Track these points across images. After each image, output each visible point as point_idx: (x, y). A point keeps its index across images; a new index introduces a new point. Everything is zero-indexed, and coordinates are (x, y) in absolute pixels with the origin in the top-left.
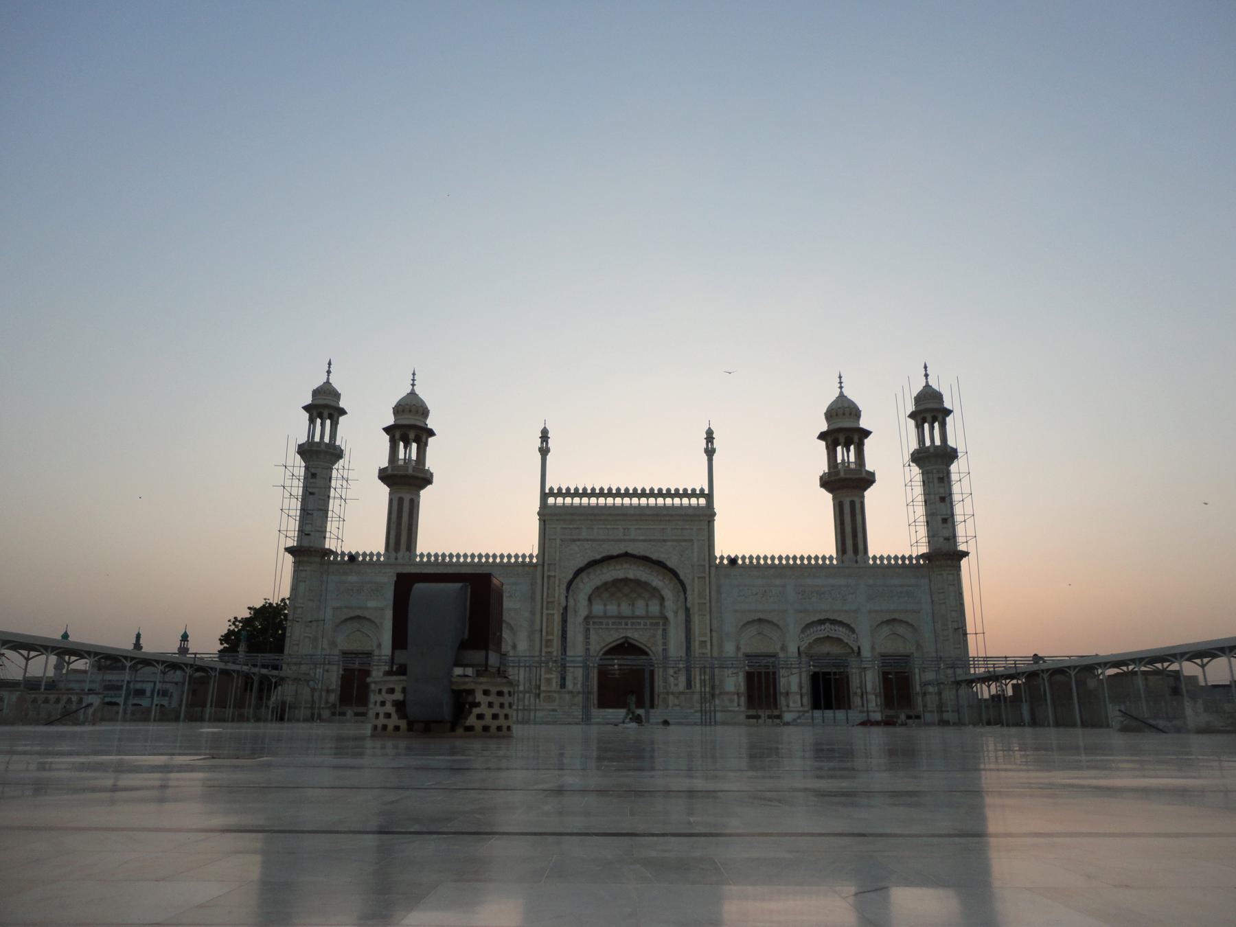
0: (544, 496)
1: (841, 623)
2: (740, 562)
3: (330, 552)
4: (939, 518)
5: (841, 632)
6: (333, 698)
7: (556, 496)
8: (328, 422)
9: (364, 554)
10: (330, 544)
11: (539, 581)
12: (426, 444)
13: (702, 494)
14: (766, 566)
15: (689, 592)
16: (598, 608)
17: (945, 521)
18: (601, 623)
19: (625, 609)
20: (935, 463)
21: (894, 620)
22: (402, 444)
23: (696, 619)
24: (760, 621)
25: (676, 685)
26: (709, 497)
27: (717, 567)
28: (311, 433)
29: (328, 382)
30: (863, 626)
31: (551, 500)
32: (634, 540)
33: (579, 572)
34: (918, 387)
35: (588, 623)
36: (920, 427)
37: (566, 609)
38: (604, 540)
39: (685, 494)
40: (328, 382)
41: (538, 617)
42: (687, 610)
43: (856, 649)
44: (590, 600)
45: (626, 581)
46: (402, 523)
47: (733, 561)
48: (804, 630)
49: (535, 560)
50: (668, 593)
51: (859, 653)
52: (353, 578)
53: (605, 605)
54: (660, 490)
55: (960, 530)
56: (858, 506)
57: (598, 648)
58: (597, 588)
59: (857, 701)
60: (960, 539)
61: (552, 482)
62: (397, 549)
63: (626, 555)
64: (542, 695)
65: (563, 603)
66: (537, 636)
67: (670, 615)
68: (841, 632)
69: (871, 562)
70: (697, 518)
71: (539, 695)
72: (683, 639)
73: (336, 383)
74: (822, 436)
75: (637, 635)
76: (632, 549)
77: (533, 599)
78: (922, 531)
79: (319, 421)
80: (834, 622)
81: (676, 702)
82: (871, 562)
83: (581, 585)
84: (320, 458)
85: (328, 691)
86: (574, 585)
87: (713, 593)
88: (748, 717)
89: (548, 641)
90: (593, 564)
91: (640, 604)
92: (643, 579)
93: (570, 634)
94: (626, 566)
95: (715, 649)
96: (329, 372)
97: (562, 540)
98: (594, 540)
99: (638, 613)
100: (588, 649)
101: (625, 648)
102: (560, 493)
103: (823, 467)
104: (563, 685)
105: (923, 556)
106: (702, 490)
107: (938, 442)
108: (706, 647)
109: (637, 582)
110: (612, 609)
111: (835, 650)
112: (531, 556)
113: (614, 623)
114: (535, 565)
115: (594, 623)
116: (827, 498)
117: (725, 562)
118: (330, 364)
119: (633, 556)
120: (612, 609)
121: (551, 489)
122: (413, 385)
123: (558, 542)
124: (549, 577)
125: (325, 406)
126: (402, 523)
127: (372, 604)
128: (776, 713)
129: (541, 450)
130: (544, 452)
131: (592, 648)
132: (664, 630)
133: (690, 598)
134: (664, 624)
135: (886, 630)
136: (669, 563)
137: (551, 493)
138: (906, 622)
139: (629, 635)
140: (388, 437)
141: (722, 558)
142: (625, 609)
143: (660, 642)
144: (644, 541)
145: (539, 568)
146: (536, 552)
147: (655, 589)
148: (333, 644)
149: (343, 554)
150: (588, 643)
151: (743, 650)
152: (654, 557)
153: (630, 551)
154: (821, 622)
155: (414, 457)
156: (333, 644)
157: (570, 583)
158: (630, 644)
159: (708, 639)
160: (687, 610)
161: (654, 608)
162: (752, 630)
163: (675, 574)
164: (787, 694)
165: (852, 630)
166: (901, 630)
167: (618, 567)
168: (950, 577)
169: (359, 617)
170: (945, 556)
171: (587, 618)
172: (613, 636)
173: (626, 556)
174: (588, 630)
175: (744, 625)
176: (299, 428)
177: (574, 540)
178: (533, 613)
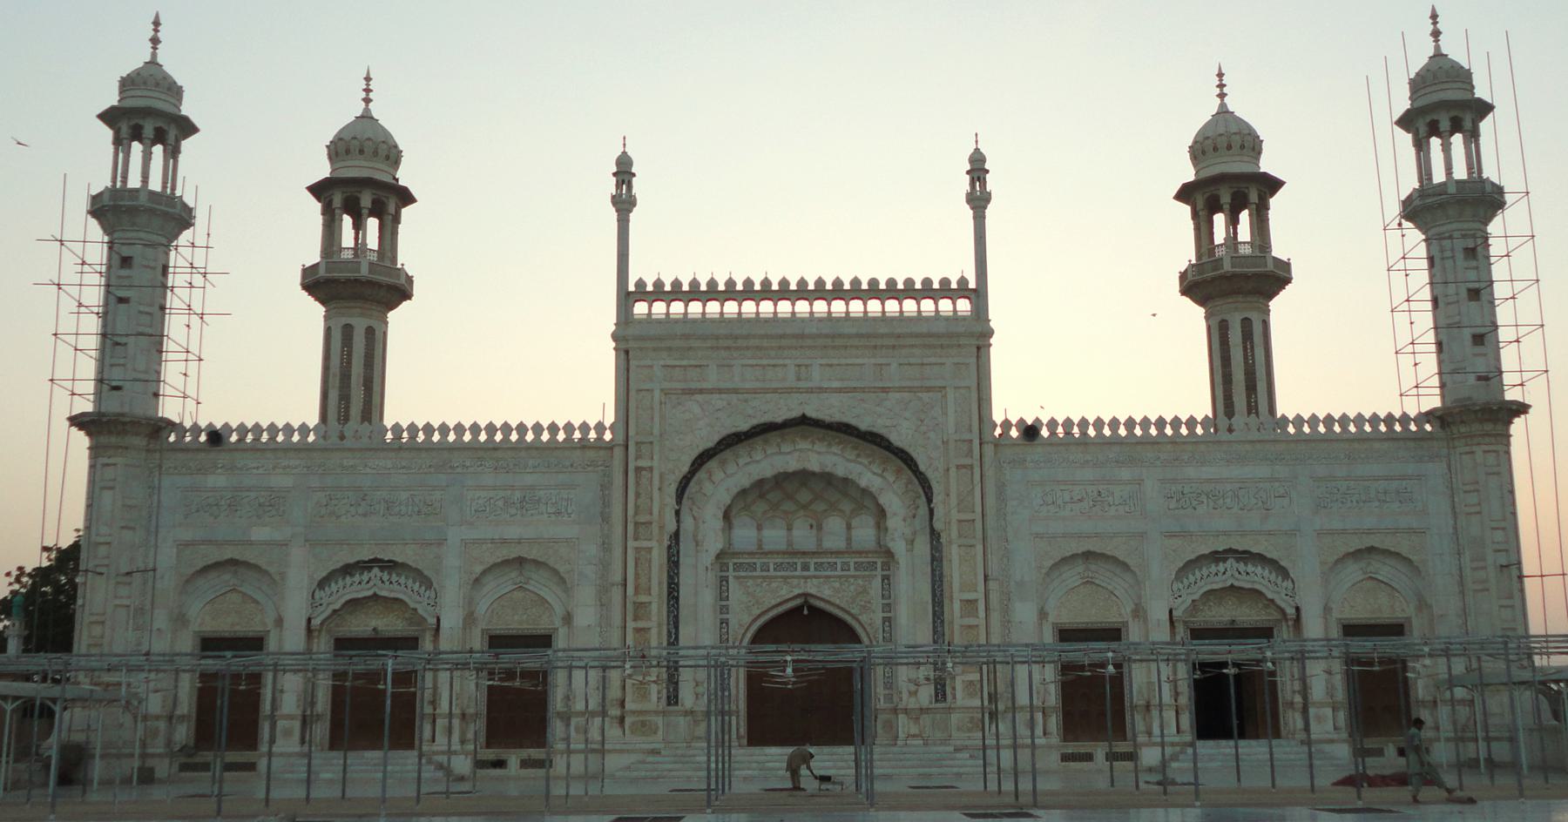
0: (626, 298)
1: (1261, 559)
2: (1045, 433)
3: (170, 425)
4: (1467, 333)
5: (1257, 577)
8: (158, 150)
9: (242, 430)
10: (169, 409)
12: (397, 219)
13: (963, 290)
14: (1101, 441)
15: (938, 499)
16: (745, 535)
17: (1479, 339)
18: (752, 567)
20: (1455, 220)
22: (347, 221)
23: (953, 553)
24: (1088, 555)
25: (913, 694)
26: (978, 295)
28: (120, 169)
32: (821, 390)
34: (1420, 58)
35: (724, 568)
36: (1421, 146)
37: (676, 536)
38: (755, 391)
40: (153, 62)
41: (617, 552)
42: (934, 535)
43: (1291, 611)
44: (727, 516)
45: (804, 477)
46: (353, 373)
47: (1030, 431)
49: (608, 436)
51: (1298, 619)
52: (218, 480)
53: (759, 528)
55: (1508, 358)
57: (747, 619)
58: (743, 492)
59: (1292, 720)
60: (1508, 379)
61: (643, 270)
63: (804, 421)
64: (628, 721)
65: (671, 526)
66: (616, 594)
67: (899, 547)
68: (1257, 577)
69: (1291, 430)
71: (622, 720)
72: (928, 598)
73: (172, 65)
75: (830, 592)
77: (605, 518)
78: (1429, 364)
79: (137, 147)
80: (1245, 556)
81: (914, 730)
82: (1291, 430)
83: (708, 487)
84: (141, 227)
86: (693, 487)
87: (991, 501)
88: (1066, 758)
89: (639, 606)
91: (834, 524)
94: (803, 445)
95: (995, 617)
96: (155, 41)
97: (666, 392)
98: (736, 391)
99: (828, 544)
100: (725, 622)
101: (804, 621)
102: (659, 293)
103: (1185, 253)
104: (673, 699)
105: (1429, 416)
106: (963, 281)
107: (1460, 173)
109: (828, 479)
110: (775, 536)
111: (1248, 615)
112: (600, 427)
113: (778, 567)
114: (610, 447)
115: (738, 567)
117: (1014, 433)
118: (157, 23)
120: (775, 536)
121: (640, 284)
122: (367, 101)
123: (657, 393)
124: (638, 470)
125: (148, 114)
126: (353, 373)
127: (261, 533)
128: (1122, 747)
129: (616, 200)
130: (624, 204)
131: (733, 623)
132: (885, 578)
134: (886, 566)
135: (1353, 572)
136: (896, 439)
137: (641, 293)
139: (813, 591)
140: (318, 206)
141: (1007, 424)
142: (803, 536)
143: (878, 603)
144: (840, 390)
145: (618, 452)
146: (609, 419)
147: (865, 492)
148: (180, 620)
149: (196, 429)
150: (724, 609)
151: (1051, 619)
152: (864, 426)
153: (812, 413)
154: (1217, 557)
155: (372, 241)
156: (180, 620)
158: (811, 608)
159: (981, 596)
160: (934, 535)
161: (864, 533)
162: (1072, 576)
163: (906, 459)
164: (1148, 707)
165: (1284, 573)
166: (1385, 570)
167: (785, 448)
168: (1491, 458)
169: (233, 562)
170: (1476, 415)
171: (720, 556)
172: (778, 593)
174: (724, 580)
175: (1056, 566)
176: (92, 161)
177: (691, 392)
178: (606, 546)
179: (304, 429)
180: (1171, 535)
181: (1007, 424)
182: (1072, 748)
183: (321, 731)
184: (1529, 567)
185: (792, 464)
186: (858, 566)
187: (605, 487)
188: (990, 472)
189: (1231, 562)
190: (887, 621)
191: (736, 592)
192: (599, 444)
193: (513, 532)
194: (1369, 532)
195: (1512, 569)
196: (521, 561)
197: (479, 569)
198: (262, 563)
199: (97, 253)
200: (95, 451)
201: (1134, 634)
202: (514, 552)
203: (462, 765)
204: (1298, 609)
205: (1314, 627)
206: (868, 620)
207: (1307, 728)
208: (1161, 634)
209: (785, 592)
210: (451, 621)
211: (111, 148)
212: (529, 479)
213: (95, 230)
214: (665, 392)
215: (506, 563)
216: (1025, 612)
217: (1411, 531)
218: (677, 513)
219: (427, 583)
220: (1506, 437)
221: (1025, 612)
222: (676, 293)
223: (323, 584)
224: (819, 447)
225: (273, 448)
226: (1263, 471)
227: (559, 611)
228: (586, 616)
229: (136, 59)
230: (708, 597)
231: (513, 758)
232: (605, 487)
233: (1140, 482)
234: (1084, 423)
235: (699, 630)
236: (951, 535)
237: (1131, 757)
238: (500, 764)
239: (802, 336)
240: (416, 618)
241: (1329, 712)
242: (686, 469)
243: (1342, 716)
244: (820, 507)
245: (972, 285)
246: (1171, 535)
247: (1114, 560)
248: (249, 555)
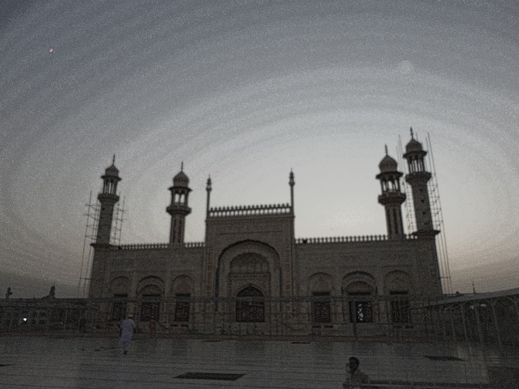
0: (208, 212)
2: (309, 242)
3: (111, 246)
7: (214, 212)
9: (125, 246)
10: (112, 242)
13: (288, 206)
16: (236, 269)
17: (424, 213)
26: (292, 208)
27: (296, 245)
29: (113, 166)
31: (211, 214)
33: (224, 251)
37: (218, 269)
39: (279, 207)
40: (113, 166)
45: (251, 254)
47: (305, 241)
50: (271, 260)
54: (274, 205)
56: (398, 211)
60: (434, 224)
61: (212, 205)
63: (249, 240)
67: (272, 271)
70: (285, 219)
73: (118, 166)
74: (378, 177)
75: (256, 283)
76: (251, 237)
80: (362, 273)
90: (231, 246)
100: (230, 291)
102: (216, 210)
104: (216, 310)
105: (414, 234)
106: (288, 204)
110: (244, 268)
116: (382, 209)
119: (253, 241)
127: (128, 270)
137: (212, 211)
141: (299, 240)
142: (251, 269)
147: (265, 258)
157: (221, 256)
171: (230, 273)
174: (231, 281)
184: (441, 275)
185: (247, 251)
189: (358, 275)
197: (174, 277)
199: (99, 208)
200: (95, 251)
201: (333, 293)
202: (182, 273)
203: (167, 326)
204: (376, 287)
205: (381, 292)
207: (379, 320)
208: (339, 294)
211: (103, 184)
213: (99, 203)
218: (219, 264)
219: (162, 281)
220: (434, 239)
221: (303, 288)
222: (220, 210)
229: (109, 164)
234: (319, 239)
235: (223, 294)
237: (331, 327)
238: (176, 325)
242: (221, 252)
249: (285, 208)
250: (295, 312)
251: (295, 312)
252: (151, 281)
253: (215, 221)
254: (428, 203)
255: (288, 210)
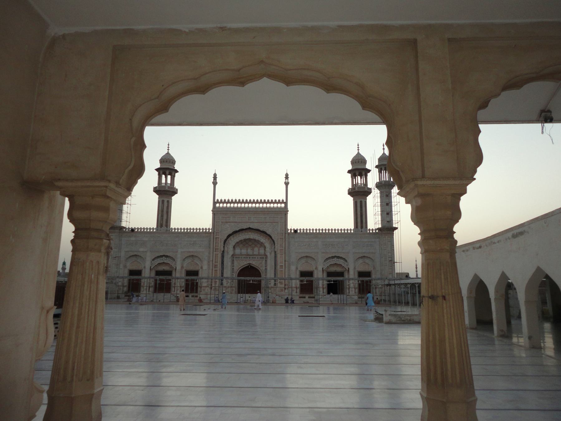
0: (215, 203)
2: (299, 231)
3: (124, 228)
4: (385, 213)
5: (341, 262)
6: (126, 289)
9: (138, 229)
10: (124, 224)
11: (212, 240)
13: (283, 202)
14: (310, 233)
16: (238, 251)
17: (388, 214)
18: (239, 258)
19: (250, 251)
21: (364, 256)
23: (279, 256)
24: (307, 257)
26: (286, 203)
27: (289, 234)
30: (351, 260)
32: (253, 222)
33: (229, 236)
35: (233, 258)
37: (223, 251)
39: (275, 202)
41: (212, 254)
42: (275, 252)
44: (234, 247)
45: (250, 240)
47: (296, 231)
48: (325, 261)
52: (133, 239)
55: (395, 218)
58: (237, 243)
61: (218, 197)
62: (161, 226)
63: (250, 228)
65: (223, 249)
66: (211, 263)
67: (268, 254)
68: (341, 262)
70: (281, 213)
75: (255, 263)
77: (210, 248)
78: (379, 218)
83: (230, 242)
85: (124, 286)
87: (287, 245)
88: (300, 297)
89: (215, 265)
90: (235, 232)
91: (256, 249)
92: (257, 239)
93: (225, 262)
94: (250, 233)
95: (287, 269)
98: (236, 222)
99: (255, 253)
104: (222, 284)
106: (283, 200)
108: (282, 268)
109: (255, 240)
110: (244, 251)
111: (339, 269)
112: (209, 229)
114: (211, 233)
115: (236, 258)
117: (293, 231)
121: (218, 200)
127: (141, 250)
128: (312, 295)
129: (213, 183)
130: (215, 183)
133: (276, 247)
135: (361, 261)
136: (268, 232)
137: (218, 202)
138: (369, 258)
141: (291, 230)
142: (250, 251)
143: (264, 265)
146: (211, 228)
147: (262, 243)
148: (125, 266)
149: (129, 228)
150: (233, 266)
152: (261, 230)
153: (251, 227)
154: (333, 257)
156: (125, 266)
160: (275, 252)
161: (262, 251)
162: (303, 261)
165: (346, 261)
166: (367, 261)
168: (389, 238)
169: (136, 255)
171: (233, 255)
172: (244, 263)
173: (250, 229)
178: (209, 253)
179: (153, 229)
180: (323, 253)
181: (291, 230)
182: (301, 295)
183: (152, 289)
186: (260, 258)
187: (210, 241)
188: (287, 240)
190: (266, 269)
191: (236, 263)
192: (209, 233)
193: (191, 250)
194: (364, 253)
195: (392, 262)
196: (193, 256)
198: (142, 255)
205: (351, 272)
206: (262, 269)
209: (245, 263)
210: (179, 268)
212: (195, 239)
214: (222, 222)
215: (190, 256)
216: (293, 268)
217: (372, 253)
219: (174, 260)
221: (293, 268)
223: (153, 260)
224: (253, 234)
225: (144, 232)
226: (343, 240)
227: (200, 266)
228: (205, 267)
230: (230, 264)
231: (190, 295)
232: (210, 241)
233: (317, 242)
236: (278, 252)
237: (314, 297)
239: (250, 211)
240: (171, 267)
241: (354, 289)
243: (357, 290)
244: (253, 246)
245: (285, 201)
246: (323, 253)
247: (311, 257)
248: (139, 254)
249: (281, 203)
250: (286, 287)
251: (286, 287)
252: (164, 260)
253: (220, 212)
254: (391, 206)
255: (283, 205)
